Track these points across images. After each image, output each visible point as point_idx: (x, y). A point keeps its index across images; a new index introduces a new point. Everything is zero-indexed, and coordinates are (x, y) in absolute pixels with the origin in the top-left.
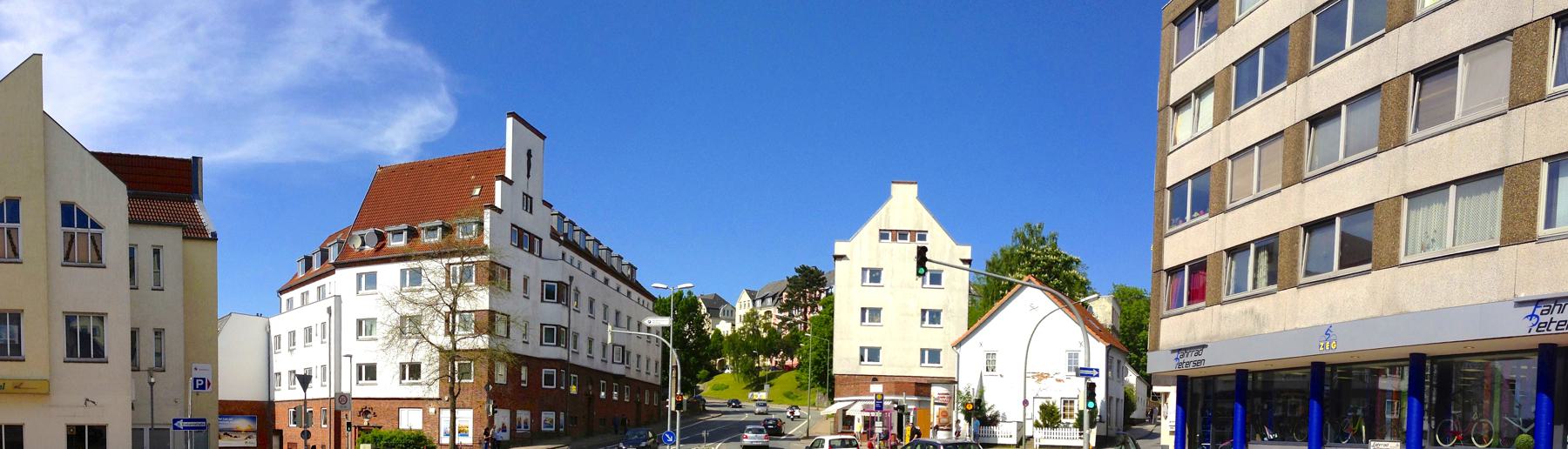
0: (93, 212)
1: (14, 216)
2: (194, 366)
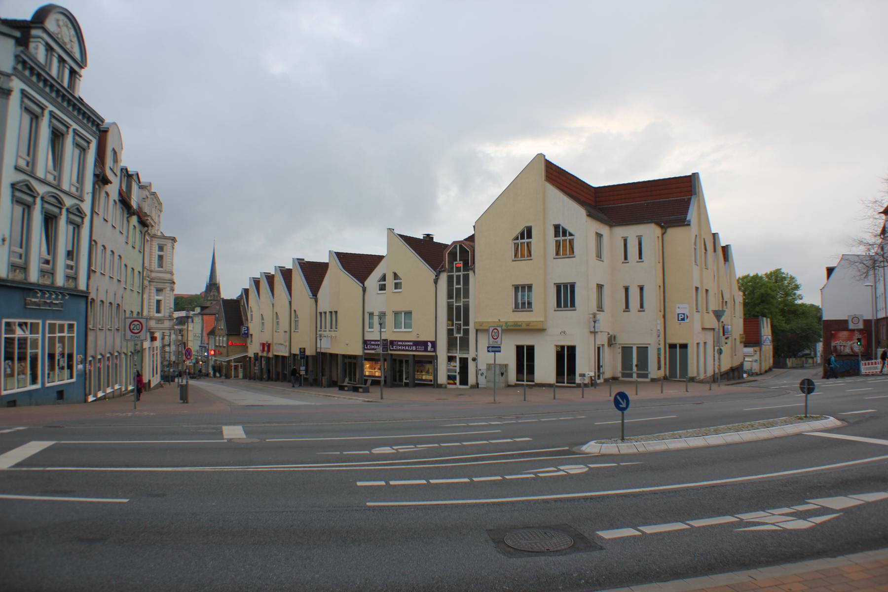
1: (530, 236)
2: (678, 305)
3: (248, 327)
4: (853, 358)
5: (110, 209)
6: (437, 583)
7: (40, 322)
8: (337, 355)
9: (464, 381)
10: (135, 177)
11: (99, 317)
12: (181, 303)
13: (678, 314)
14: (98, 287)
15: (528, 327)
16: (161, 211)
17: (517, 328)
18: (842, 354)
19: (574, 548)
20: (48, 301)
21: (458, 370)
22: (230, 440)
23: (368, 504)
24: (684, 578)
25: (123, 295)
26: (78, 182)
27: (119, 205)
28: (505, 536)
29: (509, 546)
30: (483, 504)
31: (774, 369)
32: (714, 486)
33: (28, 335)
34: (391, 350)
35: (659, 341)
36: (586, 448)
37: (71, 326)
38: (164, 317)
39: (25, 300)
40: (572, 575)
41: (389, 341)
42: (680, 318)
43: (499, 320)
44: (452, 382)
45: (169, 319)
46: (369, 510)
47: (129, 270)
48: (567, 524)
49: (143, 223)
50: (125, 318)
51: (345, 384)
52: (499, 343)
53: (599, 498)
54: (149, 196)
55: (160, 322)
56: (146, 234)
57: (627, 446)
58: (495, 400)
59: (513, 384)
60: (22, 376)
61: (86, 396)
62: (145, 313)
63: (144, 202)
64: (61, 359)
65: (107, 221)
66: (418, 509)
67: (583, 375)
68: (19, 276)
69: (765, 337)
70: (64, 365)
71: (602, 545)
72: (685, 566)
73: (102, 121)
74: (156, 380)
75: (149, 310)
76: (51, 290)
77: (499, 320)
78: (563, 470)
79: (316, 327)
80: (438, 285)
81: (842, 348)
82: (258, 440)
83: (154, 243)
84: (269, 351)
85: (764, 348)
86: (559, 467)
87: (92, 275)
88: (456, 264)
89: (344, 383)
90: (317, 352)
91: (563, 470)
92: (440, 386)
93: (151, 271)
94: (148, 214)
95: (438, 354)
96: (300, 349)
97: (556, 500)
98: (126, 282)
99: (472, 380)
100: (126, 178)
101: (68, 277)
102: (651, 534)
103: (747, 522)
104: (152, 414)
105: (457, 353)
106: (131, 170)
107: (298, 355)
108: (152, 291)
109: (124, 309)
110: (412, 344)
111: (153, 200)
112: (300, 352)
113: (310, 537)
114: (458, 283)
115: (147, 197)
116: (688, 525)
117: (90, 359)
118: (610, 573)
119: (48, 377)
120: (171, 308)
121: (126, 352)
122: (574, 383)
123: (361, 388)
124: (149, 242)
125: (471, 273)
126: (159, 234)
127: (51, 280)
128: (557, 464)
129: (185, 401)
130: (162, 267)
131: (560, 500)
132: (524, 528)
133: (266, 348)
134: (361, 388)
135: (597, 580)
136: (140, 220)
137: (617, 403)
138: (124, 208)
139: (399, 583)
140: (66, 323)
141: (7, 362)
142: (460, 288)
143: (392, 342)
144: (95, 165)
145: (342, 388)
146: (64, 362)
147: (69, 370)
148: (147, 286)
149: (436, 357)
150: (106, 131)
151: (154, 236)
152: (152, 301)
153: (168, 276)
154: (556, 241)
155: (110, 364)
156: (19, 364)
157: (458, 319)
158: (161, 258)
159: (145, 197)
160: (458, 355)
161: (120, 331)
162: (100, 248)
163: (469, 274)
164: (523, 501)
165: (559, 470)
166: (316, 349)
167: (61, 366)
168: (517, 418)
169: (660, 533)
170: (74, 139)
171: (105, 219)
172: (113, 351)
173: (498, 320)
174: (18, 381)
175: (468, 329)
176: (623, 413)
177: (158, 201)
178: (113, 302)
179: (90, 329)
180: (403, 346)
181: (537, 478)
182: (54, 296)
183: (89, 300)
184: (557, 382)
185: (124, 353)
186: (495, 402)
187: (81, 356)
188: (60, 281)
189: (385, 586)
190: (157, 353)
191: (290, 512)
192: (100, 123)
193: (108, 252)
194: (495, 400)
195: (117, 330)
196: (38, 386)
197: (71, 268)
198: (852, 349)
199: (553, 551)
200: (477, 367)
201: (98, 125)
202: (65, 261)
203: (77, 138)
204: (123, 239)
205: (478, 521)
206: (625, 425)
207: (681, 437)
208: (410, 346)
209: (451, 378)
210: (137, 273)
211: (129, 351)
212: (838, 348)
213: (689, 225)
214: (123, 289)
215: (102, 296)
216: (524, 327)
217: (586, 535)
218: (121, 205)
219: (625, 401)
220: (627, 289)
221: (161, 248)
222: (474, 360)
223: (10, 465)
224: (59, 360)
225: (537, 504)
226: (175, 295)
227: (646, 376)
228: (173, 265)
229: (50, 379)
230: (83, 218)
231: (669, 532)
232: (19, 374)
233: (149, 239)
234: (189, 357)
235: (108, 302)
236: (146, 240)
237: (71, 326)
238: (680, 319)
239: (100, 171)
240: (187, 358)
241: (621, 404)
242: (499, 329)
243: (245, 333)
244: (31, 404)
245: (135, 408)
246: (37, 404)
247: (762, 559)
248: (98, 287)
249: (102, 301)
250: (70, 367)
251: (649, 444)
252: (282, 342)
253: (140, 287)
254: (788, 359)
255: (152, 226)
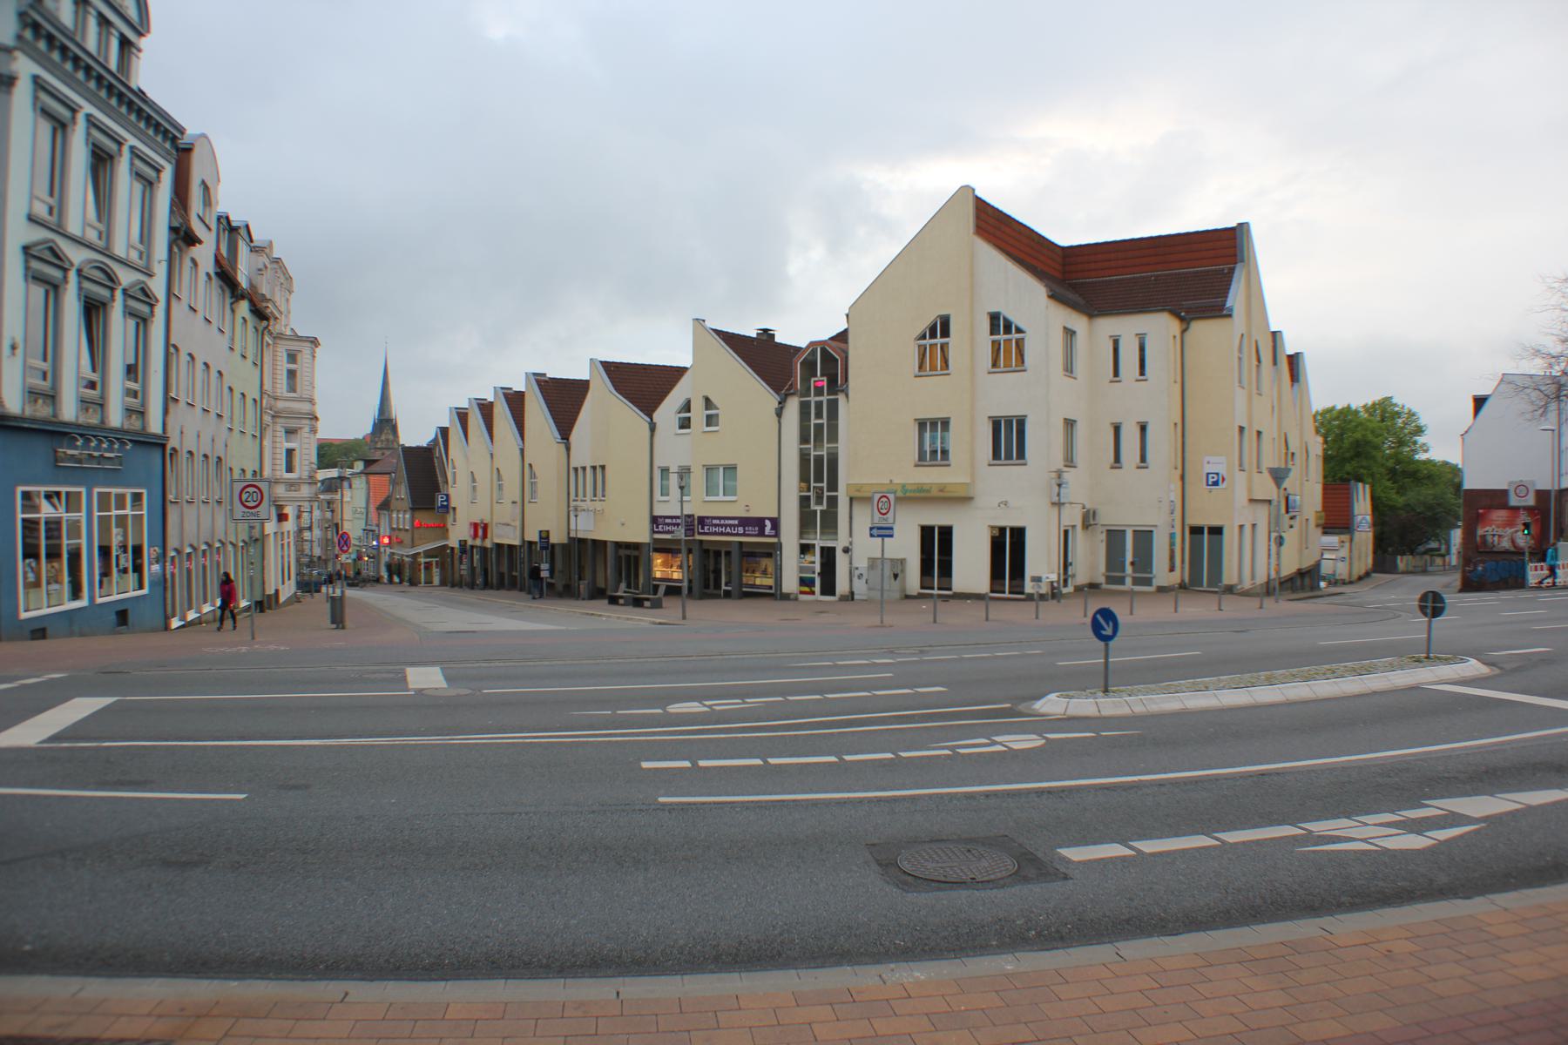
0: (1017, 320)
1: (946, 333)
2: (1207, 459)
3: (447, 496)
4: (1515, 558)
5: (201, 289)
6: (781, 934)
7: (83, 490)
8: (605, 542)
9: (829, 587)
10: (243, 232)
11: (186, 480)
12: (329, 454)
13: (1208, 474)
14: (182, 427)
15: (941, 494)
16: (290, 292)
17: (923, 495)
18: (1495, 549)
19: (1019, 877)
20: (96, 454)
21: (818, 568)
22: (420, 691)
23: (661, 799)
24: (1208, 930)
25: (226, 442)
26: (142, 242)
27: (215, 282)
28: (899, 855)
29: (904, 871)
30: (861, 801)
31: (1374, 575)
32: (1263, 774)
33: (61, 513)
34: (699, 534)
35: (1173, 520)
36: (1041, 706)
37: (137, 498)
38: (300, 479)
39: (56, 452)
40: (1014, 921)
41: (696, 517)
42: (1211, 480)
43: (891, 481)
44: (806, 589)
45: (309, 483)
46: (664, 810)
47: (237, 396)
48: (1006, 836)
49: (260, 314)
50: (232, 481)
51: (619, 594)
52: (891, 521)
53: (1063, 791)
54: (269, 266)
55: (293, 488)
56: (266, 332)
57: (1113, 702)
58: (882, 622)
59: (915, 594)
60: (54, 586)
61: (167, 619)
62: (267, 473)
63: (259, 277)
64: (122, 556)
65: (195, 311)
66: (747, 808)
67: (1037, 579)
68: (42, 411)
69: (1360, 517)
70: (126, 566)
71: (1067, 872)
72: (1209, 909)
73: (182, 131)
74: (288, 590)
75: (274, 467)
76: (100, 434)
77: (891, 481)
78: (1000, 744)
79: (569, 494)
80: (783, 417)
81: (1496, 538)
82: (469, 692)
83: (279, 350)
84: (485, 536)
85: (1357, 535)
86: (993, 738)
87: (171, 405)
88: (815, 382)
89: (617, 592)
90: (570, 538)
91: (1000, 744)
92: (786, 597)
93: (276, 399)
94: (268, 297)
95: (784, 539)
96: (541, 532)
97: (987, 795)
98: (232, 418)
99: (842, 585)
100: (227, 232)
101: (129, 411)
102: (1153, 855)
103: (1319, 836)
104: (282, 648)
105: (816, 539)
106: (236, 219)
107: (536, 543)
108: (278, 434)
109: (229, 465)
110: (736, 522)
111: (276, 272)
112: (541, 538)
113: (561, 857)
114: (819, 415)
115: (266, 267)
116: (1217, 839)
117: (173, 554)
118: (1079, 920)
119: (101, 586)
120: (312, 463)
121: (234, 542)
122: (1022, 593)
123: (647, 599)
124: (271, 347)
125: (841, 398)
126: (289, 332)
127: (99, 417)
128: (990, 732)
129: (341, 626)
130: (294, 390)
131: (995, 794)
132: (931, 841)
133: (480, 532)
134: (647, 599)
135: (1058, 931)
136: (253, 308)
137: (1096, 628)
138: (226, 288)
139: (715, 934)
140: (128, 492)
141: (27, 561)
142: (823, 424)
143: (702, 520)
144: (171, 212)
145: (614, 600)
146: (127, 561)
147: (136, 574)
148: (268, 425)
149: (779, 546)
150: (188, 150)
151: (279, 337)
152: (278, 451)
153: (305, 407)
154: (993, 342)
155: (208, 563)
156: (49, 565)
157: (819, 479)
158: (292, 374)
159: (261, 266)
160: (819, 542)
161: (224, 504)
162: (184, 358)
163: (836, 400)
164: (930, 796)
165: (994, 743)
166: (569, 533)
167: (121, 567)
168: (921, 652)
169: (1168, 853)
170: (132, 164)
171: (191, 307)
172: (213, 542)
173: (888, 482)
174: (48, 594)
175: (836, 497)
176: (1107, 645)
177: (284, 274)
178: (210, 455)
179: (171, 502)
180: (722, 526)
181: (955, 757)
182: (105, 446)
183: (168, 451)
184: (992, 591)
185: (231, 543)
186: (882, 625)
187: (156, 548)
188: (115, 418)
189: (691, 938)
190: (289, 543)
191: (526, 814)
192: (178, 135)
193: (199, 366)
194: (882, 622)
195: (218, 502)
196: (83, 603)
197: (135, 394)
198: (1513, 541)
199: (982, 882)
200: (851, 563)
201: (174, 139)
202: (124, 384)
203: (137, 162)
204: (224, 342)
205: (852, 830)
206: (1110, 666)
207: (1207, 689)
208: (734, 526)
209: (806, 582)
210: (252, 402)
211: (240, 538)
212: (1489, 539)
213: (1230, 316)
214: (226, 431)
215: (189, 443)
216: (935, 493)
217: (1040, 855)
218: (221, 283)
219: (1111, 624)
220: (1117, 429)
221: (292, 357)
222: (846, 550)
223: (39, 740)
224: (117, 557)
225: (955, 802)
226: (319, 439)
227: (1148, 582)
228: (314, 387)
229: (102, 590)
230: (152, 306)
231: (1184, 851)
232: (48, 583)
233: (270, 342)
234: (345, 548)
235: (202, 453)
236: (265, 344)
237: (137, 498)
238: (1210, 483)
239: (181, 221)
240: (341, 549)
241: (1105, 630)
242: (891, 497)
243: (442, 505)
244: (71, 634)
245: (253, 638)
246: (82, 635)
247: (1343, 899)
248: (182, 427)
249: (190, 453)
250: (138, 569)
251: (1151, 699)
252: (509, 521)
253: (256, 427)
254: (1399, 557)
255: (276, 318)
